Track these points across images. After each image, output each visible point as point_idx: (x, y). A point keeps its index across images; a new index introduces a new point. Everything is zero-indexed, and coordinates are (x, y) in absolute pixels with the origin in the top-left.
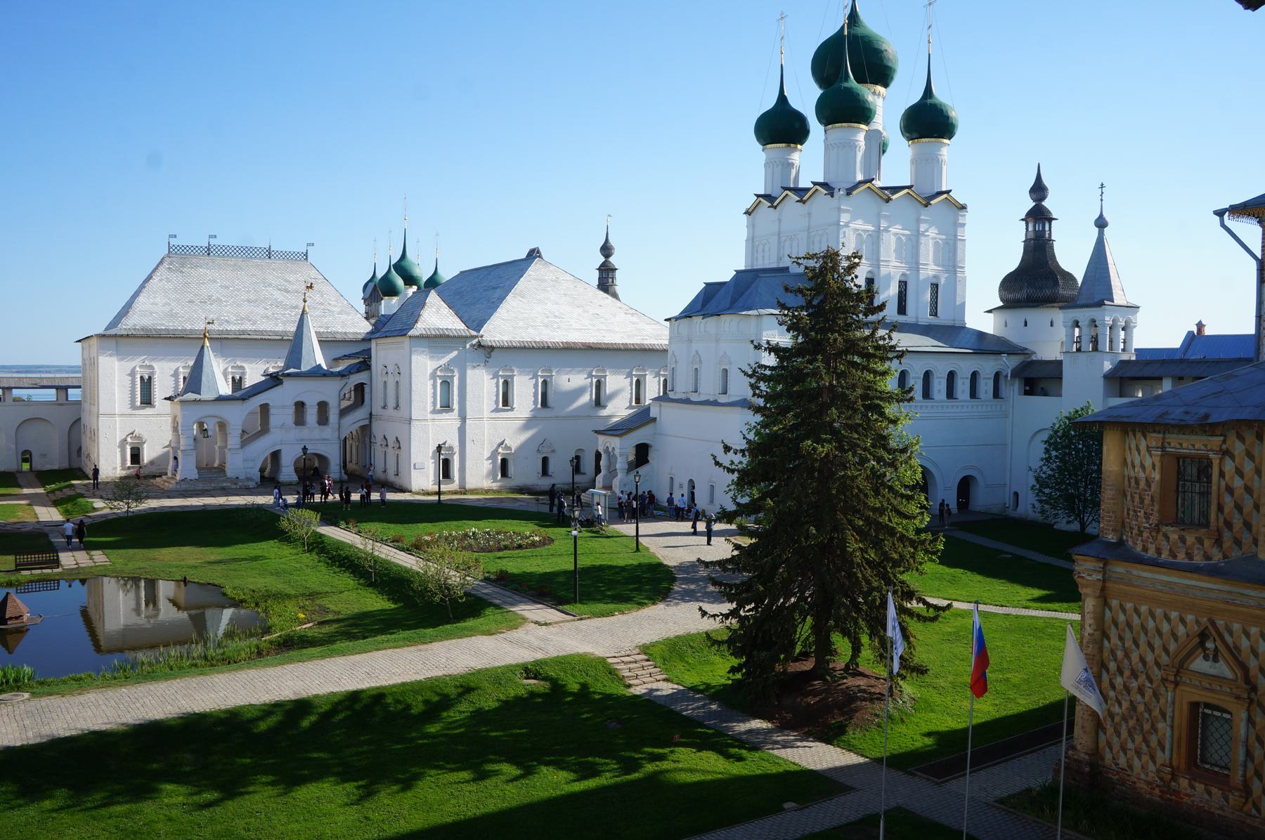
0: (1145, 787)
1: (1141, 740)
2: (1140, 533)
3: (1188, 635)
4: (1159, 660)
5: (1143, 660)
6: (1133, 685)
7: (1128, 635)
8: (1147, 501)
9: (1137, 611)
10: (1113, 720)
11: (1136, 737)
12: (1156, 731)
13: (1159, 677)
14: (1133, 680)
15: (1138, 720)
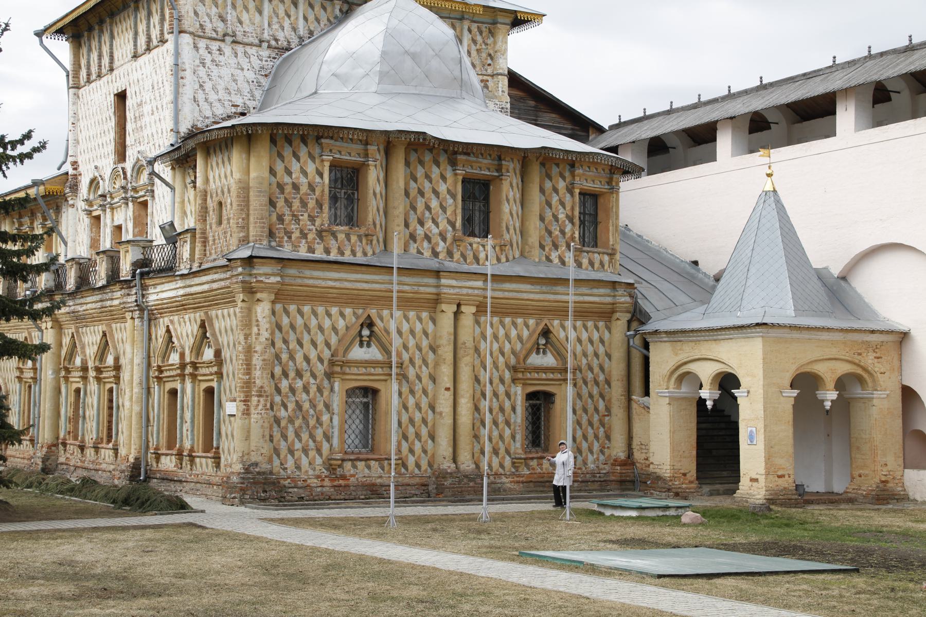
0: (316, 481)
1: (308, 436)
2: (304, 235)
3: (347, 328)
4: (321, 356)
5: (307, 359)
6: (299, 385)
7: (292, 337)
8: (312, 204)
9: (300, 312)
10: (279, 425)
11: (302, 435)
12: (321, 425)
13: (323, 371)
14: (298, 380)
15: (304, 418)
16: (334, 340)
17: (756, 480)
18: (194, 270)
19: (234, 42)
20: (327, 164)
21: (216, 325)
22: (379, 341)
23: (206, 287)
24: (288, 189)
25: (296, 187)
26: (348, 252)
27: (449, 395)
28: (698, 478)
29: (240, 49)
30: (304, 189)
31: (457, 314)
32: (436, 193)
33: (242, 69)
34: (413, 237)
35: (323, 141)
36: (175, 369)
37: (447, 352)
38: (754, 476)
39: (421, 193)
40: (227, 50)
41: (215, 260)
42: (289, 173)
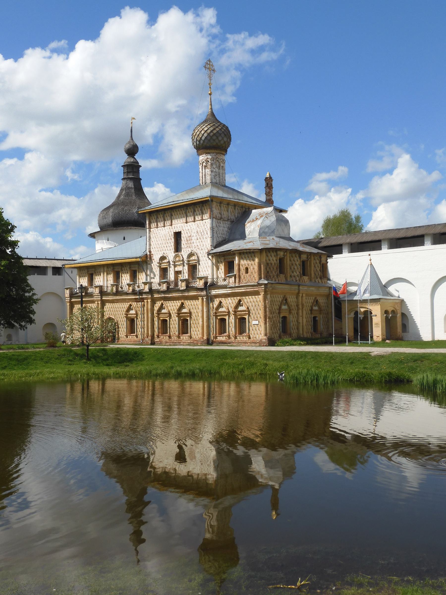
2: (274, 277)
5: (275, 309)
16: (279, 304)
17: (379, 337)
18: (237, 285)
19: (223, 220)
20: (278, 258)
21: (246, 300)
22: (288, 304)
23: (244, 290)
24: (270, 264)
25: (271, 264)
26: (282, 281)
27: (301, 317)
28: (354, 338)
29: (224, 222)
30: (273, 264)
31: (302, 296)
32: (296, 264)
33: (225, 228)
34: (291, 276)
35: (278, 252)
36: (225, 313)
37: (300, 307)
38: (378, 336)
39: (292, 265)
40: (222, 222)
41: (246, 283)
42: (269, 260)
